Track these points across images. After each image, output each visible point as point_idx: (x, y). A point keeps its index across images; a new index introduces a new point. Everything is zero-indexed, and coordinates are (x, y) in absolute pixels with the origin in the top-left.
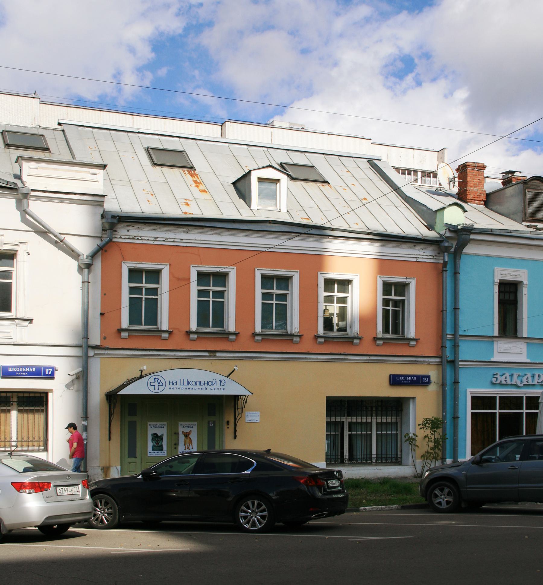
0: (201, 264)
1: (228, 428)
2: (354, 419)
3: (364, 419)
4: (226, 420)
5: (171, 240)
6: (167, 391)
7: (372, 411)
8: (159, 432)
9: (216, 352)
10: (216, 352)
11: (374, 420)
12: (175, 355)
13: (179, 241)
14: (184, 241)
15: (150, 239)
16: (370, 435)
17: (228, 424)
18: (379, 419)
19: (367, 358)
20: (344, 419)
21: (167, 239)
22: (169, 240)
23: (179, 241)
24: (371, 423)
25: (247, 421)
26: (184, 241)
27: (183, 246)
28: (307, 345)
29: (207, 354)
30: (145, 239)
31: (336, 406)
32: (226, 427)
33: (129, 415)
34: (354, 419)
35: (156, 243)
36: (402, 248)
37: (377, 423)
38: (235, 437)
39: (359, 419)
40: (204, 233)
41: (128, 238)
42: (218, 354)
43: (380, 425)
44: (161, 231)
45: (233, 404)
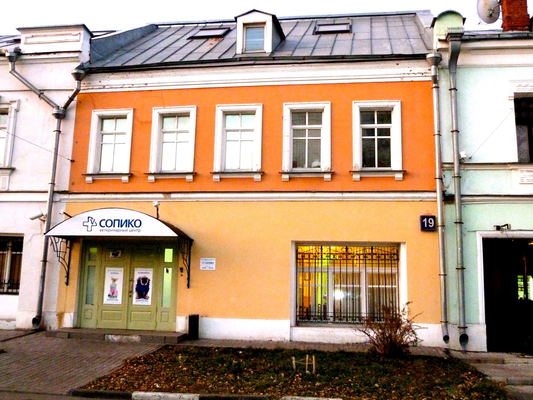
0: (164, 105)
1: (182, 275)
5: (137, 86)
8: (115, 276)
10: (170, 193)
12: (131, 198)
13: (144, 85)
14: (148, 85)
15: (118, 86)
17: (182, 272)
19: (340, 195)
21: (133, 85)
23: (144, 85)
25: (201, 268)
29: (161, 196)
32: (180, 273)
41: (99, 88)
42: (173, 196)
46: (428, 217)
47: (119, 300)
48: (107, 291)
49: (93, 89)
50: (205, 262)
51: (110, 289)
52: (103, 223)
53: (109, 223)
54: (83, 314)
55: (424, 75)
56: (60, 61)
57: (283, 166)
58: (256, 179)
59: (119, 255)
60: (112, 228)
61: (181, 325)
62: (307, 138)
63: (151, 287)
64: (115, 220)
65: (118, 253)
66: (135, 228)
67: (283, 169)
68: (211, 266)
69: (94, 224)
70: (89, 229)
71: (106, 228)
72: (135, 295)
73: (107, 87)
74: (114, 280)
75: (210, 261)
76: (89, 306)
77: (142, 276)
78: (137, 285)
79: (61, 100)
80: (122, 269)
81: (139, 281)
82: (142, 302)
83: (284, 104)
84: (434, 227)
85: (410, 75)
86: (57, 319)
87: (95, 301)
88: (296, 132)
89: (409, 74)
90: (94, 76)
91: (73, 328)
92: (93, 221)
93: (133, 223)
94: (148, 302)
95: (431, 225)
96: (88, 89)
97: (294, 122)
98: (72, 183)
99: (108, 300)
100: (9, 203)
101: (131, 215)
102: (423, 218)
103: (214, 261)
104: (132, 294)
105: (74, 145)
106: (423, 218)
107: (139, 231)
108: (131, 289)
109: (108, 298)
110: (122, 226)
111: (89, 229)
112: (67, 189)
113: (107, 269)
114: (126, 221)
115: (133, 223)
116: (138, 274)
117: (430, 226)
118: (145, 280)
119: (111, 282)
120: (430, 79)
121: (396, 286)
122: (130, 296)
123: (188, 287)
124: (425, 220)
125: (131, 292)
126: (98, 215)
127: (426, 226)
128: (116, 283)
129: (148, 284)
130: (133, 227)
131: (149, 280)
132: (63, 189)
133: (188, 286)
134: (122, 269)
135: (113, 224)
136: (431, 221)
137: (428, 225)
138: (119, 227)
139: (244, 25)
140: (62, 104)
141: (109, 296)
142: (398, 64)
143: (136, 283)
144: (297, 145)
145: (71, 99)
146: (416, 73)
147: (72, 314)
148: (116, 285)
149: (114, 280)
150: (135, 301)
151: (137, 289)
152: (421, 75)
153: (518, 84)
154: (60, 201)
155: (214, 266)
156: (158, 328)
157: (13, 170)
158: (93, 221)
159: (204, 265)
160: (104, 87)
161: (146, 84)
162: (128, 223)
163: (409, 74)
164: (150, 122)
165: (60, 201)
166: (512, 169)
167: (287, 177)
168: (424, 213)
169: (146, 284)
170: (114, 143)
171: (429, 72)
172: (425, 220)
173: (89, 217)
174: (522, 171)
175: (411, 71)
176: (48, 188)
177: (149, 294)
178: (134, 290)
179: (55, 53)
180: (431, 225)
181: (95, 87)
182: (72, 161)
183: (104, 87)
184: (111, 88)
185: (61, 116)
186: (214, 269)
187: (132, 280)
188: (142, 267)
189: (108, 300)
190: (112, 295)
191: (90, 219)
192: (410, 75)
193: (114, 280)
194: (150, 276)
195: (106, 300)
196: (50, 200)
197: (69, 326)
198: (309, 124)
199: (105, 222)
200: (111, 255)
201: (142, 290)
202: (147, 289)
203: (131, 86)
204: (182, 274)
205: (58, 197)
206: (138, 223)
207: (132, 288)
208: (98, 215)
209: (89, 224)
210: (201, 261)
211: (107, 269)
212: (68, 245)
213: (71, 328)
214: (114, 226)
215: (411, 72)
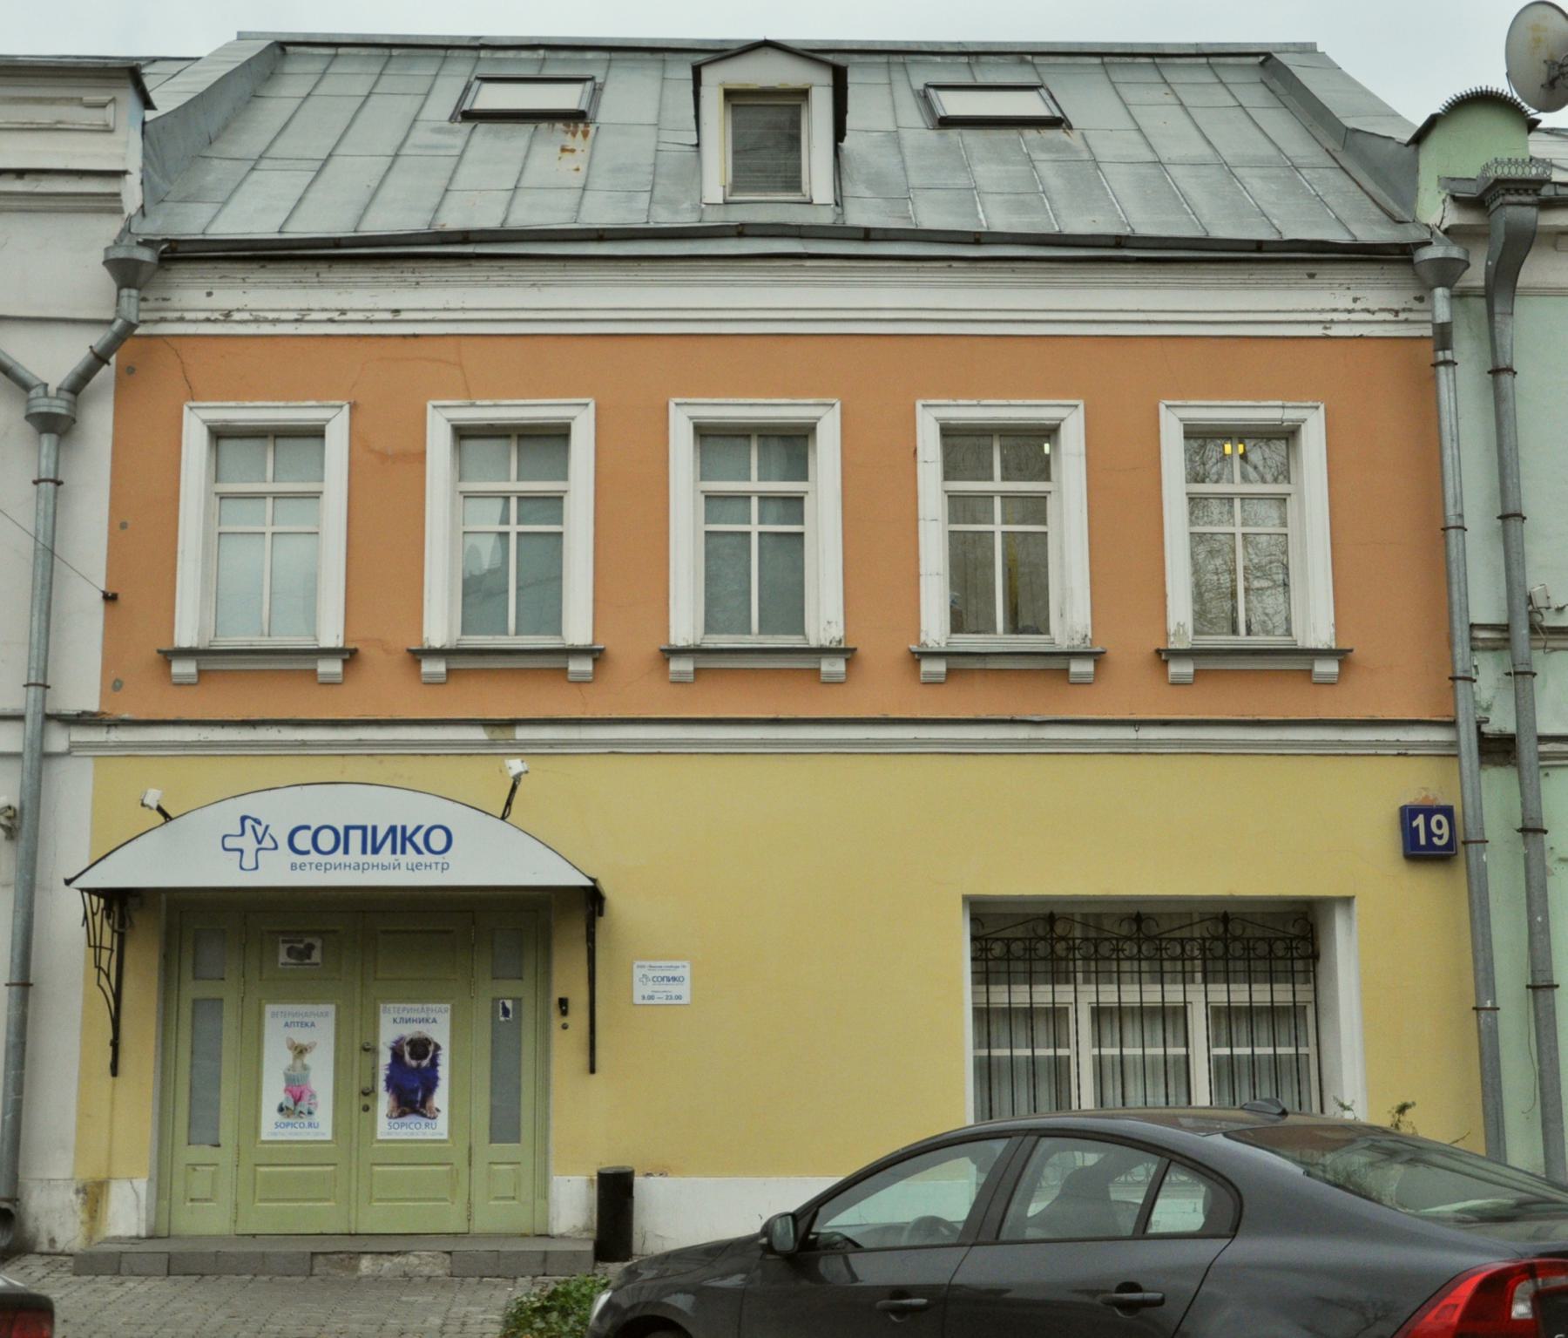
0: (469, 393)
1: (565, 1027)
2: (1109, 995)
3: (1152, 995)
4: (556, 995)
5: (360, 316)
6: (277, 871)
8: (302, 1037)
9: (513, 723)
10: (513, 723)
11: (1198, 999)
12: (360, 743)
13: (389, 316)
14: (403, 316)
15: (284, 316)
17: (564, 1013)
18: (1219, 994)
20: (1064, 994)
21: (343, 312)
23: (389, 316)
24: (1182, 1012)
25: (637, 1000)
26: (403, 316)
27: (404, 336)
29: (479, 734)
30: (266, 321)
31: (1019, 941)
32: (556, 1021)
34: (1109, 995)
36: (1259, 286)
39: (1131, 995)
40: (476, 284)
42: (522, 733)
43: (1225, 1018)
44: (322, 284)
45: (583, 931)
46: (1429, 812)
47: (321, 1125)
48: (273, 1092)
49: (181, 320)
50: (651, 974)
51: (283, 1085)
52: (303, 840)
53: (326, 840)
54: (178, 1187)
55: (1402, 316)
56: (34, 204)
57: (924, 627)
58: (829, 674)
59: (316, 956)
60: (339, 856)
61: (571, 1207)
62: (998, 528)
63: (443, 1071)
64: (347, 829)
65: (310, 947)
66: (428, 857)
67: (923, 638)
68: (674, 989)
69: (268, 843)
70: (249, 862)
71: (314, 857)
72: (384, 1101)
73: (236, 316)
75: (670, 974)
76: (202, 1153)
77: (409, 1031)
78: (392, 1067)
79: (52, 360)
80: (331, 1008)
81: (397, 1054)
82: (413, 1129)
83: (919, 403)
84: (1450, 845)
85: (1354, 317)
86: (78, 1207)
87: (226, 1134)
88: (960, 506)
89: (1349, 311)
91: (149, 1238)
92: (260, 830)
93: (419, 839)
94: (439, 1128)
95: (1440, 837)
96: (163, 320)
97: (951, 471)
98: (113, 685)
99: (277, 1125)
101: (411, 811)
102: (1408, 813)
103: (684, 971)
104: (376, 1099)
105: (111, 533)
106: (1408, 813)
107: (445, 867)
108: (367, 1084)
109: (278, 1117)
110: (376, 851)
111: (249, 862)
112: (93, 706)
113: (269, 1009)
114: (393, 829)
115: (419, 839)
116: (394, 1026)
117: (1435, 840)
118: (421, 1047)
119: (288, 1057)
120: (1428, 331)
121: (1312, 1050)
122: (366, 1109)
125: (369, 1092)
126: (282, 810)
127: (1423, 841)
128: (308, 1059)
129: (434, 1063)
130: (419, 851)
131: (437, 1047)
133: (592, 1070)
134: (331, 1008)
136: (1439, 825)
137: (1428, 841)
138: (364, 851)
139: (729, 94)
141: (281, 1109)
142: (1312, 276)
143: (385, 1059)
145: (100, 358)
146: (1373, 307)
147: (142, 1185)
148: (305, 1068)
149: (297, 1048)
150: (387, 1126)
151: (391, 1083)
152: (1390, 317)
154: (68, 753)
155: (684, 990)
156: (482, 1224)
158: (260, 830)
159: (649, 989)
160: (227, 316)
161: (397, 311)
162: (400, 838)
163: (1349, 311)
164: (421, 456)
165: (68, 753)
167: (939, 667)
168: (1410, 798)
169: (425, 1063)
170: (269, 529)
171: (1417, 305)
173: (243, 819)
175: (1355, 300)
177: (440, 1098)
178: (382, 1085)
179: (20, 173)
180: (1440, 837)
182: (110, 598)
183: (227, 316)
184: (256, 321)
186: (686, 1000)
187: (370, 1050)
188: (410, 1000)
189: (277, 1125)
191: (248, 823)
192: (1354, 317)
193: (300, 1051)
194: (439, 1032)
195: (271, 1126)
196: (32, 749)
197: (133, 1233)
198: (1005, 478)
199: (309, 834)
200: (283, 957)
201: (412, 1086)
202: (429, 1081)
203: (335, 315)
204: (566, 1020)
205: (59, 739)
206: (438, 839)
207: (374, 1077)
208: (282, 810)
209: (248, 843)
210: (638, 973)
211: (269, 1009)
213: (138, 1237)
214: (346, 851)
215: (1358, 306)
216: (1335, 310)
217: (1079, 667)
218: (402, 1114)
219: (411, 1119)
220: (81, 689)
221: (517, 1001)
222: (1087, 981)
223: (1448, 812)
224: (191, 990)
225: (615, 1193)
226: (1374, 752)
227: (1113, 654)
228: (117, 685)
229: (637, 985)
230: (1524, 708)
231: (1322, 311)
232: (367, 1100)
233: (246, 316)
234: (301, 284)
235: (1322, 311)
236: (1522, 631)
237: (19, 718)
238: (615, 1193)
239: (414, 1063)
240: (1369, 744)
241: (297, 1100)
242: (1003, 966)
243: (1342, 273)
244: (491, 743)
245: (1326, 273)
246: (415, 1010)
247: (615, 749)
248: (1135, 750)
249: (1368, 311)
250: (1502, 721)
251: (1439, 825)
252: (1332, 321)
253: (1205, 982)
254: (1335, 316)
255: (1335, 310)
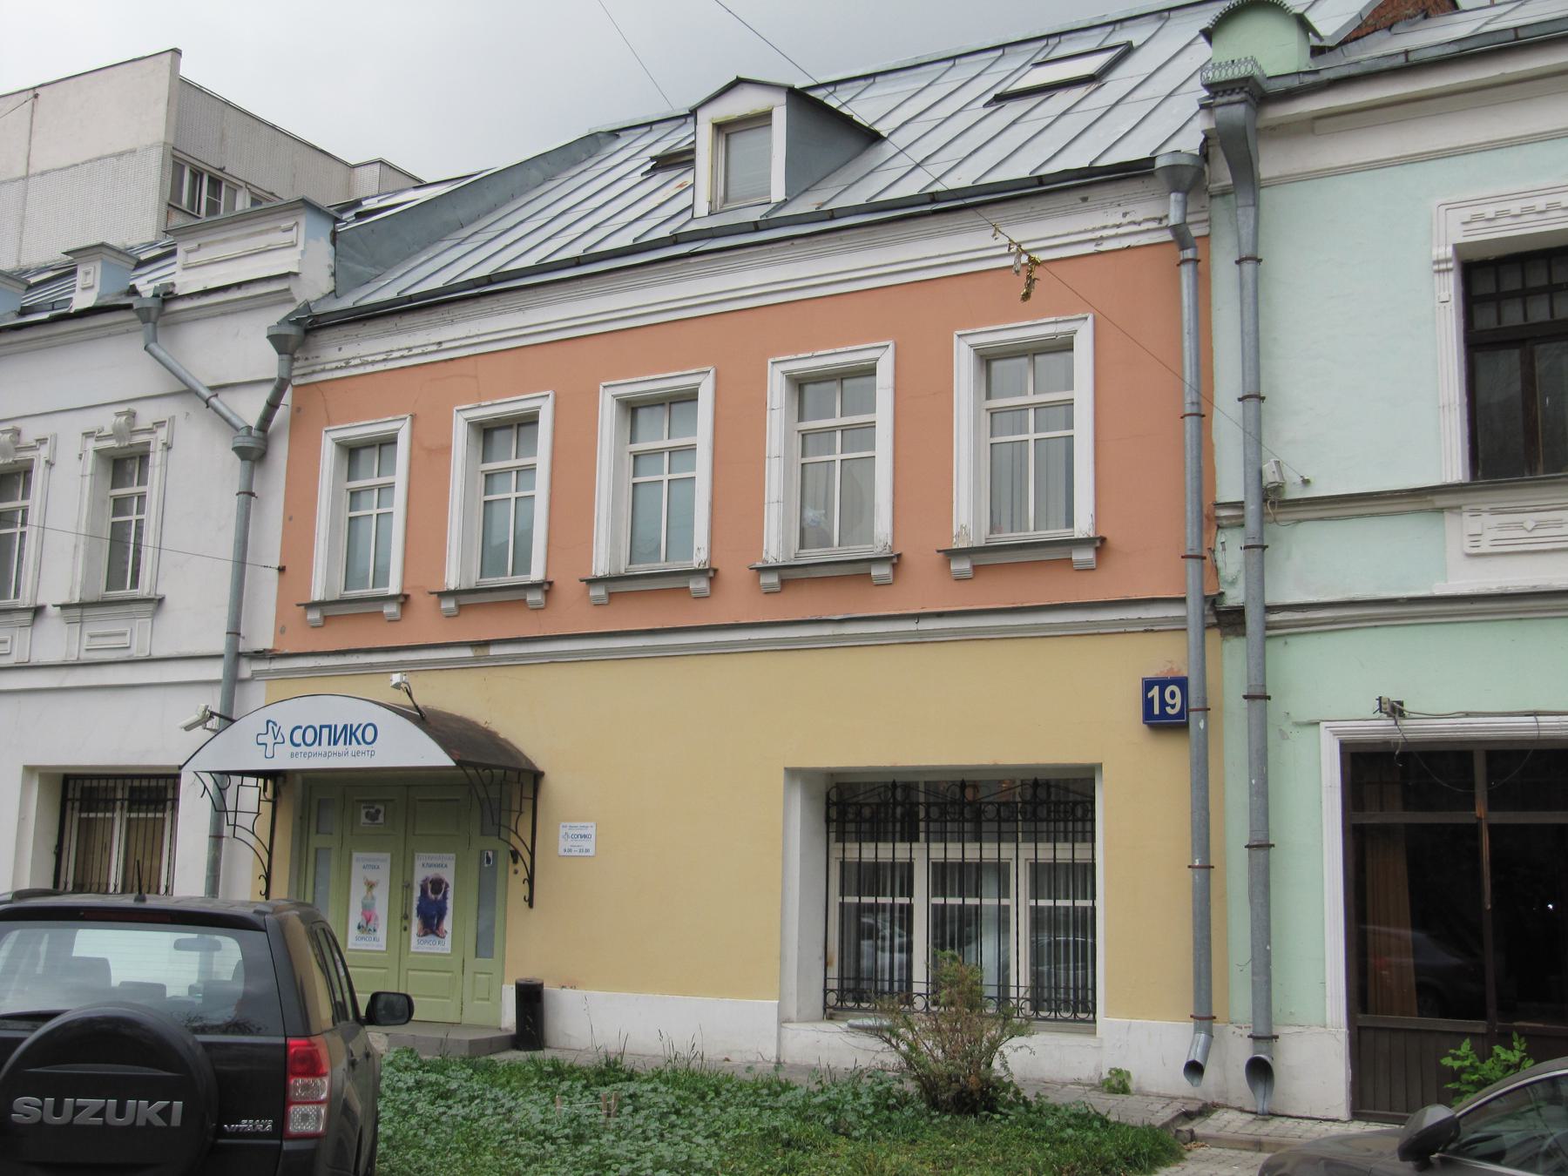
7: (978, 818)
8: (372, 876)
9: (487, 644)
10: (487, 644)
14: (445, 346)
16: (908, 910)
17: (515, 862)
21: (410, 349)
22: (415, 351)
23: (435, 348)
25: (561, 852)
26: (445, 346)
28: (736, 602)
29: (467, 653)
30: (368, 363)
33: (482, 834)
35: (390, 365)
37: (1035, 867)
38: (530, 902)
42: (494, 651)
46: (1163, 683)
48: (355, 917)
49: (323, 370)
52: (298, 737)
59: (381, 819)
63: (450, 904)
65: (378, 811)
66: (364, 747)
69: (280, 739)
71: (303, 748)
72: (416, 924)
73: (353, 362)
74: (371, 886)
75: (583, 832)
77: (431, 873)
79: (249, 408)
80: (388, 855)
84: (1180, 715)
89: (1118, 226)
90: (324, 336)
95: (1173, 706)
96: (314, 372)
98: (281, 630)
100: (161, 691)
102: (1148, 685)
103: (592, 831)
106: (1148, 685)
112: (269, 646)
113: (355, 855)
114: (345, 727)
116: (422, 872)
117: (1169, 710)
118: (437, 885)
120: (1167, 236)
123: (531, 905)
124: (1155, 692)
125: (406, 917)
126: (291, 714)
127: (1157, 711)
128: (375, 892)
129: (445, 897)
132: (260, 647)
134: (388, 855)
135: (318, 737)
136: (1173, 695)
137: (1168, 711)
140: (253, 419)
142: (1085, 199)
143: (417, 893)
144: (807, 483)
145: (273, 405)
146: (1139, 218)
150: (418, 944)
153: (1466, 214)
155: (590, 845)
157: (160, 601)
161: (440, 343)
162: (349, 733)
164: (446, 450)
166: (1441, 510)
167: (773, 579)
172: (1155, 692)
174: (1476, 513)
175: (1125, 215)
176: (219, 644)
177: (447, 924)
178: (415, 912)
179: (239, 285)
180: (1173, 706)
181: (328, 366)
182: (281, 570)
185: (254, 453)
186: (592, 853)
187: (408, 886)
190: (366, 927)
193: (371, 886)
194: (448, 876)
200: (363, 819)
202: (441, 914)
203: (405, 353)
205: (246, 669)
206: (369, 735)
208: (291, 714)
209: (269, 739)
210: (562, 832)
212: (269, 794)
215: (1125, 221)
216: (1105, 227)
217: (880, 571)
218: (425, 934)
219: (431, 937)
220: (262, 636)
221: (495, 852)
222: (902, 840)
223: (1182, 683)
224: (316, 841)
225: (530, 998)
226: (1122, 630)
227: (908, 555)
228: (283, 631)
229: (561, 840)
230: (1258, 579)
231: (1094, 230)
232: (405, 923)
233: (357, 361)
234: (388, 333)
235: (1094, 230)
236: (1252, 508)
237: (220, 656)
238: (530, 998)
239: (433, 896)
240: (1065, 625)
241: (368, 921)
242: (994, 826)
243: (1110, 192)
244: (476, 659)
245: (1095, 194)
246: (435, 858)
247: (553, 660)
248: (921, 640)
249: (1134, 223)
250: (1234, 596)
251: (1173, 695)
252: (1102, 238)
253: (928, 841)
254: (1105, 233)
255: (1105, 227)
